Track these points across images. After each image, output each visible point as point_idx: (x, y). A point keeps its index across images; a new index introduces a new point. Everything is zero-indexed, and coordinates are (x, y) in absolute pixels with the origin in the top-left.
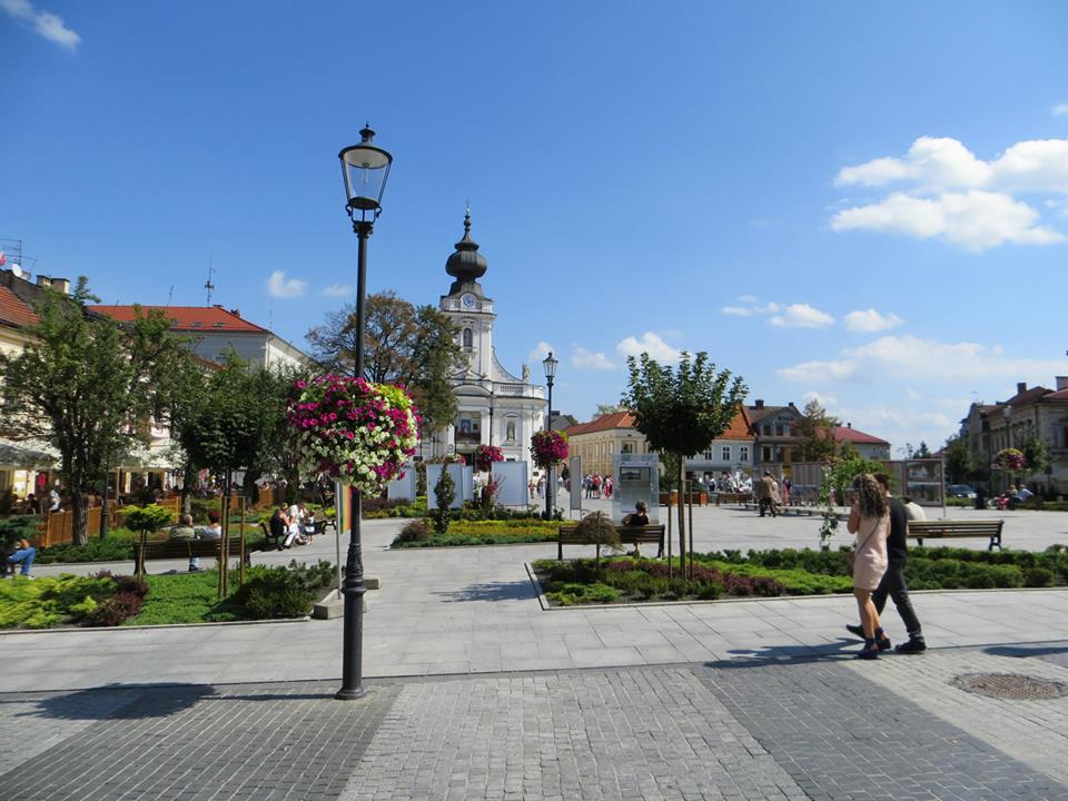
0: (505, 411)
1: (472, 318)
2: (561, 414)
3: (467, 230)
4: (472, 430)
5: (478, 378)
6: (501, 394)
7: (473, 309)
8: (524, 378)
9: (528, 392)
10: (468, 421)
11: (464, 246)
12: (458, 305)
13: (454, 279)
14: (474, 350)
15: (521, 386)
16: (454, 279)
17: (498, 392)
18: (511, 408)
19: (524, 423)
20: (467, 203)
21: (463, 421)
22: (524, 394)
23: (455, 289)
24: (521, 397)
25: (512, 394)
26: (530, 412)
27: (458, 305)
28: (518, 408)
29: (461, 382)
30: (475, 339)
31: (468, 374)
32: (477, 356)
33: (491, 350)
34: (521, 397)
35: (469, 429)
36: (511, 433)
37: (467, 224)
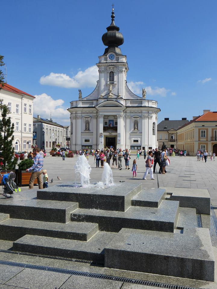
0: (132, 114)
1: (113, 65)
3: (113, 20)
4: (115, 125)
5: (116, 97)
6: (130, 105)
7: (114, 61)
8: (143, 96)
9: (146, 104)
10: (113, 121)
11: (112, 28)
12: (106, 59)
13: (107, 47)
14: (115, 83)
16: (107, 47)
17: (129, 104)
19: (143, 121)
20: (113, 6)
21: (110, 121)
22: (143, 105)
23: (106, 51)
24: (141, 107)
25: (136, 105)
27: (106, 59)
28: (140, 113)
29: (106, 100)
31: (110, 95)
32: (116, 86)
33: (124, 82)
34: (141, 107)
35: (113, 125)
36: (136, 126)
37: (113, 17)
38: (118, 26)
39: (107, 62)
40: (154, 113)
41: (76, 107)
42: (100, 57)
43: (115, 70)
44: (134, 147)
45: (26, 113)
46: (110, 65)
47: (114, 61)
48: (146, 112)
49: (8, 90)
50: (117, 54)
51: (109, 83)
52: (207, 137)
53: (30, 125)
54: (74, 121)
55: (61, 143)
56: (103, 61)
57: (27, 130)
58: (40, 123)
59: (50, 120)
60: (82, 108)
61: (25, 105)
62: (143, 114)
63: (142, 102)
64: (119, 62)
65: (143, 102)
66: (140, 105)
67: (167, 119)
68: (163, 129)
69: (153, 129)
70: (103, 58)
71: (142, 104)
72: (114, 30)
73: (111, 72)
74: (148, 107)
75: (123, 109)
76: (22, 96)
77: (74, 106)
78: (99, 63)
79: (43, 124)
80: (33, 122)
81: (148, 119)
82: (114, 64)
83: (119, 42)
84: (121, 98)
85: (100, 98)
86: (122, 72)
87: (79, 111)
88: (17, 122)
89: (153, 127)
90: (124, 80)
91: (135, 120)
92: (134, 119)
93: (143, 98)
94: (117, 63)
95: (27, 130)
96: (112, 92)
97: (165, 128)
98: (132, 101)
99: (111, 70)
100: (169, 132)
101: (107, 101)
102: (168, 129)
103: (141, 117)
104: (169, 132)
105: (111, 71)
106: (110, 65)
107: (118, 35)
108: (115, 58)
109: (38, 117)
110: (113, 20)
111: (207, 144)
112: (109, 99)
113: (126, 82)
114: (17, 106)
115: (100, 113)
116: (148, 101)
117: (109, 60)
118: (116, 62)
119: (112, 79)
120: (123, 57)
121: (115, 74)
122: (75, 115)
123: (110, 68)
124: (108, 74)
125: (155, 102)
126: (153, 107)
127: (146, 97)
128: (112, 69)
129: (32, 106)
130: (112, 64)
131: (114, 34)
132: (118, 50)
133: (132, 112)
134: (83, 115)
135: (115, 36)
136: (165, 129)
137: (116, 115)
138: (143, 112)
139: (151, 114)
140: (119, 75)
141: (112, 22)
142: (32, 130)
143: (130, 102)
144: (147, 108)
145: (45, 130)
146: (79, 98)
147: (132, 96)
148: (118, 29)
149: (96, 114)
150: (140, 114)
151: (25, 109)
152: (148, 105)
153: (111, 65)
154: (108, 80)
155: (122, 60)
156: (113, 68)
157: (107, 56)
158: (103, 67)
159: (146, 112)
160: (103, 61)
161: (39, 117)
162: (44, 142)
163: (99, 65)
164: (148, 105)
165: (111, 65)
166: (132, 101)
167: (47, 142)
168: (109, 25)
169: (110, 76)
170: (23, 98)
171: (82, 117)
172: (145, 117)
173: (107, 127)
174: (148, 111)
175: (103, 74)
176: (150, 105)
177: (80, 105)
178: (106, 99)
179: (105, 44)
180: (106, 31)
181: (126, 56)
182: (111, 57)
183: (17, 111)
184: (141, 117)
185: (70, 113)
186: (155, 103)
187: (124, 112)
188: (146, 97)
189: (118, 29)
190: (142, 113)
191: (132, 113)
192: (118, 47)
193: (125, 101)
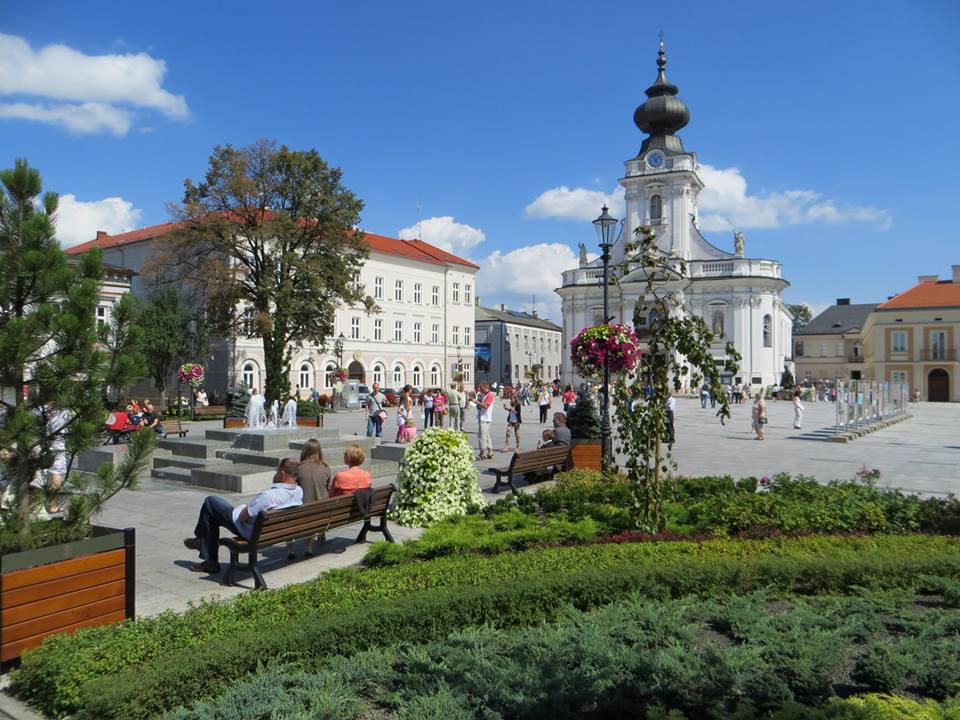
1: (659, 181)
2: (852, 303)
3: (660, 70)
6: (703, 275)
7: (662, 169)
8: (737, 251)
11: (657, 91)
12: (642, 167)
13: (647, 136)
14: (666, 222)
15: (730, 262)
16: (647, 136)
18: (718, 293)
19: (736, 313)
22: (735, 273)
24: (731, 277)
26: (744, 297)
27: (642, 167)
28: (727, 292)
30: (665, 209)
33: (688, 219)
34: (731, 277)
36: (718, 325)
37: (661, 63)
38: (674, 83)
39: (646, 173)
40: (768, 289)
41: (574, 285)
42: (627, 163)
43: (664, 191)
45: (458, 304)
46: (650, 181)
47: (662, 169)
48: (743, 289)
49: (418, 258)
50: (669, 153)
51: (649, 223)
52: (911, 351)
53: (468, 330)
54: (569, 317)
55: (549, 367)
56: (635, 172)
57: (461, 340)
58: (499, 323)
59: (531, 314)
60: (586, 288)
61: (456, 285)
62: (735, 295)
63: (732, 265)
64: (673, 169)
65: (735, 264)
66: (727, 273)
67: (843, 302)
68: (829, 329)
69: (765, 333)
70: (635, 165)
72: (662, 95)
73: (654, 197)
74: (750, 277)
75: (684, 286)
76: (444, 268)
77: (570, 282)
78: (626, 177)
79: (508, 325)
80: (476, 321)
81: (749, 308)
82: (664, 176)
83: (676, 122)
86: (680, 194)
87: (580, 293)
88: (418, 322)
89: (765, 327)
90: (687, 215)
91: (714, 310)
93: (737, 255)
94: (669, 175)
95: (461, 340)
97: (838, 326)
98: (708, 264)
99: (655, 191)
100: (848, 337)
102: (843, 329)
103: (729, 302)
104: (848, 337)
105: (652, 196)
106: (650, 181)
107: (673, 104)
108: (664, 161)
109: (503, 309)
110: (660, 70)
111: (910, 369)
114: (435, 289)
115: (627, 297)
116: (750, 262)
117: (649, 170)
118: (666, 170)
119: (656, 213)
120: (684, 159)
121: (663, 201)
122: (571, 303)
123: (651, 187)
124: (648, 204)
125: (769, 262)
126: (763, 275)
127: (743, 254)
128: (656, 188)
129: (473, 289)
130: (657, 177)
131: (661, 106)
132: (671, 142)
133: (708, 290)
134: (589, 302)
135: (664, 110)
136: (837, 330)
138: (736, 290)
139: (758, 293)
140: (675, 202)
141: (660, 76)
142: (472, 341)
144: (747, 279)
145: (512, 340)
146: (581, 263)
147: (706, 251)
148: (672, 91)
149: (619, 300)
150: (728, 296)
151: (456, 295)
152: (750, 270)
153: (655, 181)
154: (648, 217)
155: (680, 164)
156: (659, 187)
157: (645, 159)
158: (636, 187)
159: (743, 289)
160: (635, 172)
161: (505, 307)
162: (508, 368)
163: (626, 180)
164: (750, 270)
165: (655, 181)
166: (708, 264)
167: (517, 366)
168: (651, 83)
169: (653, 207)
170: (449, 272)
171: (587, 306)
172: (740, 303)
173: (645, 330)
174: (751, 288)
175: (635, 204)
176: (756, 270)
177: (583, 279)
179: (644, 131)
180: (644, 99)
181: (691, 155)
182: (655, 162)
183: (435, 300)
184: (729, 302)
185: (561, 299)
186: (771, 266)
187: (688, 291)
188: (743, 254)
189: (672, 91)
190: (733, 292)
191: (708, 293)
192: (677, 133)
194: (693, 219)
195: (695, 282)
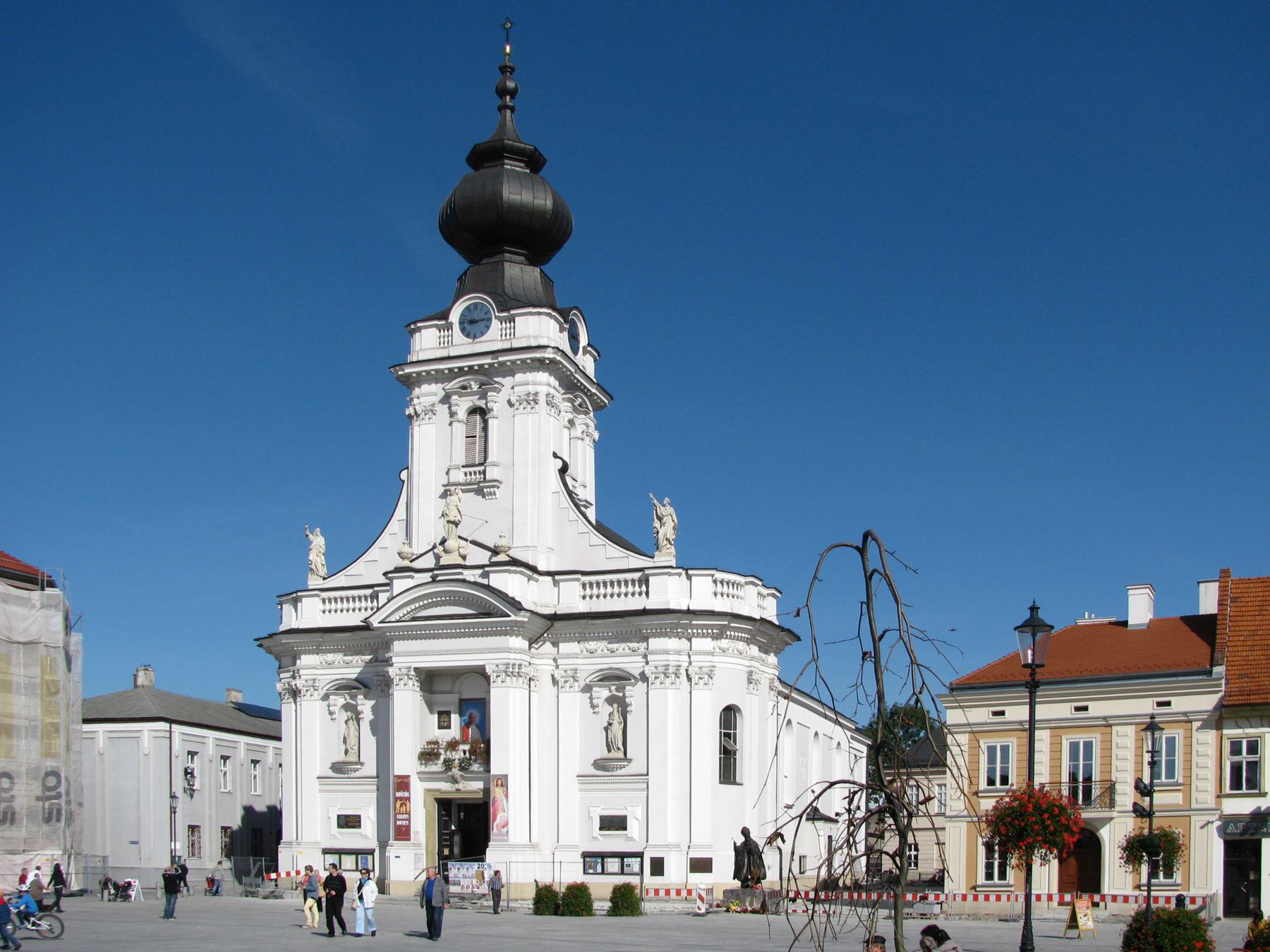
22: (651, 604)
44: (603, 856)
63: (646, 581)
71: (647, 594)
73: (474, 411)
74: (689, 612)
84: (514, 562)
85: (398, 570)
92: (602, 693)
96: (461, 531)
101: (434, 580)
112: (443, 575)
113: (559, 464)
124: (460, 430)
126: (717, 609)
137: (483, 667)
143: (584, 586)
174: (690, 640)
178: (430, 574)
193: (549, 579)
194: (564, 470)
195: (558, 624)
